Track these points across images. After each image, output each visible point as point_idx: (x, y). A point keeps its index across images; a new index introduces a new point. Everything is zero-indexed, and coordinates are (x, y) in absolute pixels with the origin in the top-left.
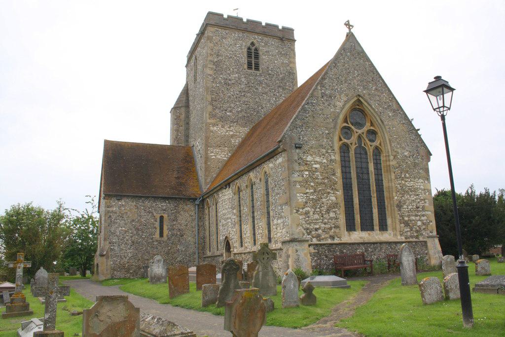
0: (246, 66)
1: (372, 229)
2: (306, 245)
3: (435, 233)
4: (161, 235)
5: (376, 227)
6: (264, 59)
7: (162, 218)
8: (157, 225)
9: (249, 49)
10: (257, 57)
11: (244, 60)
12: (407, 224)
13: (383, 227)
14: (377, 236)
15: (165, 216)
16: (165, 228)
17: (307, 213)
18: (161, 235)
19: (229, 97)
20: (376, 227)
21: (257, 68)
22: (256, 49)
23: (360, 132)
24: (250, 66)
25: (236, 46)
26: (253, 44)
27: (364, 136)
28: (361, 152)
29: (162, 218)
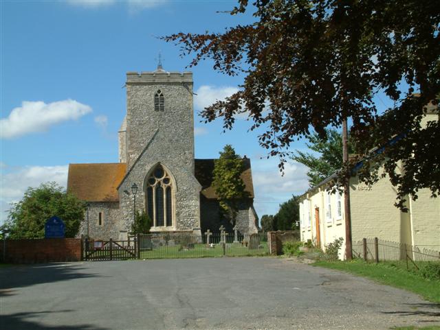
0: (154, 109)
1: (162, 225)
2: (126, 233)
3: (199, 227)
4: (100, 224)
5: (165, 224)
6: (168, 101)
7: (100, 214)
8: (98, 218)
9: (157, 95)
10: (163, 100)
11: (153, 105)
12: (182, 223)
13: (169, 223)
14: (165, 228)
15: (102, 212)
16: (102, 219)
17: (128, 220)
18: (100, 224)
19: (142, 133)
20: (165, 224)
21: (162, 110)
22: (162, 95)
23: (159, 180)
24: (157, 109)
25: (146, 95)
26: (159, 91)
27: (162, 183)
28: (159, 189)
29: (100, 214)
